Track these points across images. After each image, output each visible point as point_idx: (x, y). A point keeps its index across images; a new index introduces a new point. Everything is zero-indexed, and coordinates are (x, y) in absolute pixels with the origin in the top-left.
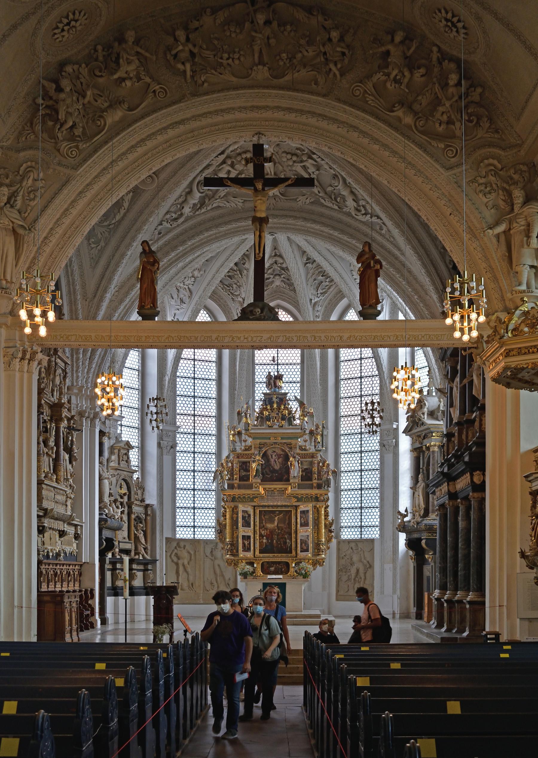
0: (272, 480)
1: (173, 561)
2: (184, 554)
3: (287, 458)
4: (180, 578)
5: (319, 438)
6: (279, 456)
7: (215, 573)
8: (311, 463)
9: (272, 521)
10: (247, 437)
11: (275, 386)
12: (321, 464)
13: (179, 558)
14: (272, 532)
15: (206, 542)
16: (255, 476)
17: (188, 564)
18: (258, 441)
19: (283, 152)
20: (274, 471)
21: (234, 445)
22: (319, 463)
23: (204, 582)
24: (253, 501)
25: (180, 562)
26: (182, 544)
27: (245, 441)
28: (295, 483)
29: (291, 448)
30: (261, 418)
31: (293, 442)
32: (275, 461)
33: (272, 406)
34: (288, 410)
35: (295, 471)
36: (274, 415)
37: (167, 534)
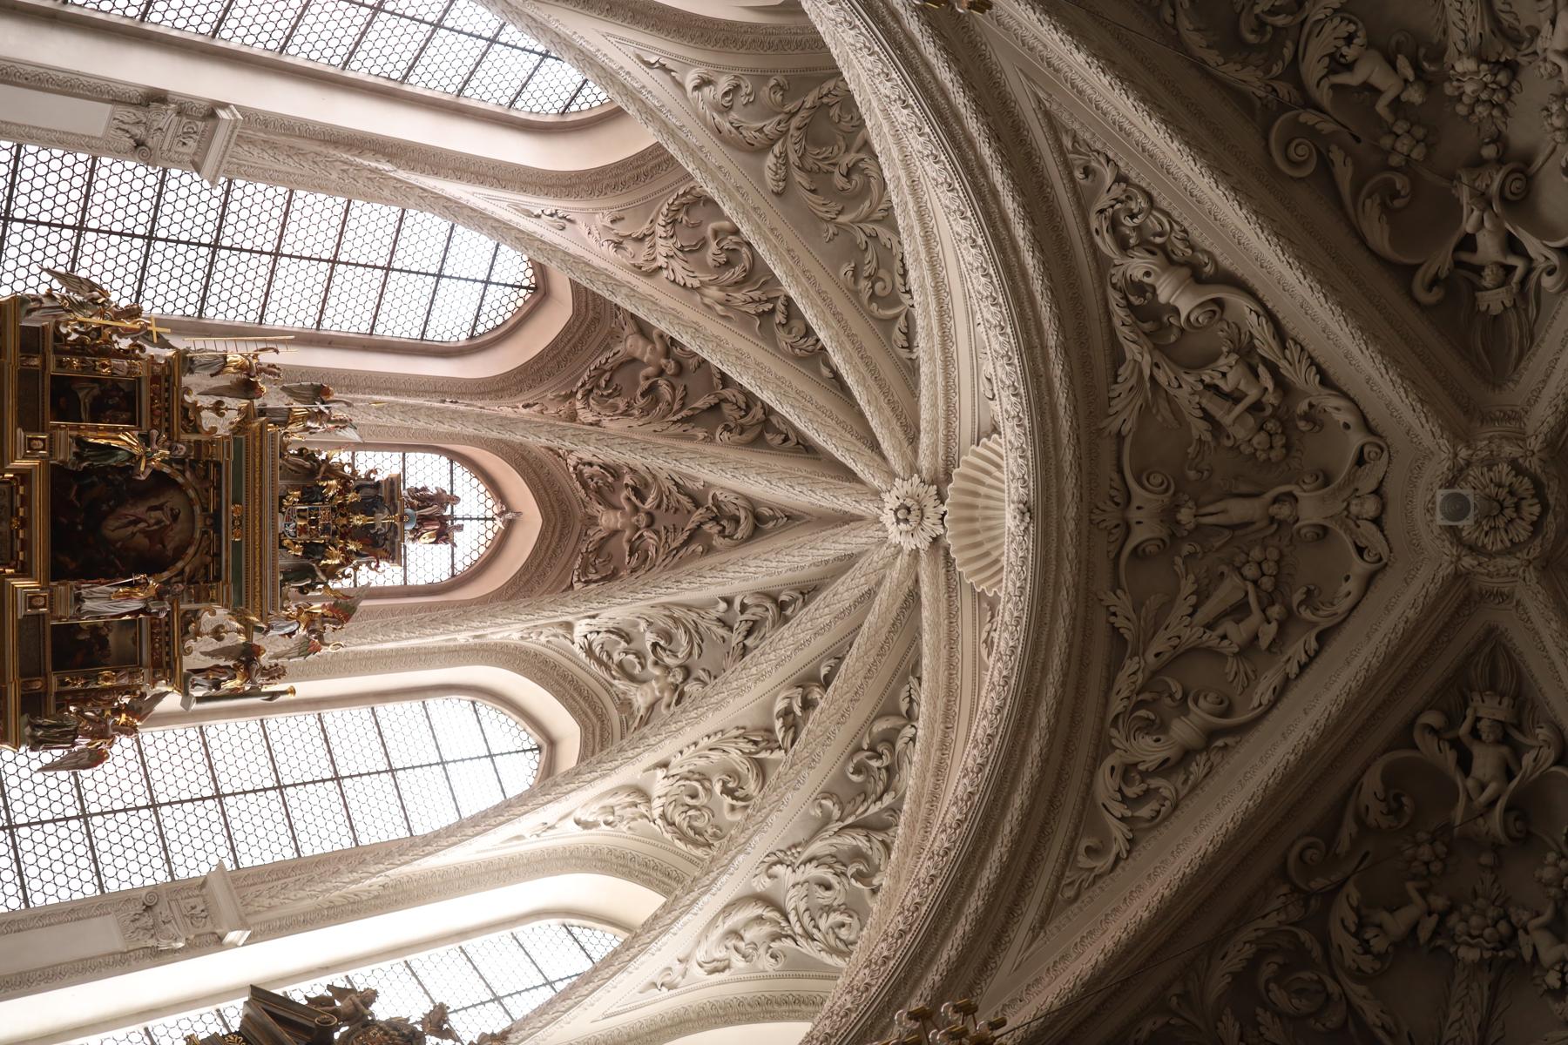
5: (230, 685)
8: (129, 662)
10: (233, 416)
11: (423, 520)
12: (126, 700)
16: (80, 442)
18: (226, 458)
19: (1282, 555)
21: (206, 366)
22: (126, 690)
27: (217, 408)
28: (50, 601)
29: (191, 580)
30: (310, 474)
31: (225, 588)
33: (356, 508)
34: (341, 565)
35: (106, 602)
36: (324, 514)
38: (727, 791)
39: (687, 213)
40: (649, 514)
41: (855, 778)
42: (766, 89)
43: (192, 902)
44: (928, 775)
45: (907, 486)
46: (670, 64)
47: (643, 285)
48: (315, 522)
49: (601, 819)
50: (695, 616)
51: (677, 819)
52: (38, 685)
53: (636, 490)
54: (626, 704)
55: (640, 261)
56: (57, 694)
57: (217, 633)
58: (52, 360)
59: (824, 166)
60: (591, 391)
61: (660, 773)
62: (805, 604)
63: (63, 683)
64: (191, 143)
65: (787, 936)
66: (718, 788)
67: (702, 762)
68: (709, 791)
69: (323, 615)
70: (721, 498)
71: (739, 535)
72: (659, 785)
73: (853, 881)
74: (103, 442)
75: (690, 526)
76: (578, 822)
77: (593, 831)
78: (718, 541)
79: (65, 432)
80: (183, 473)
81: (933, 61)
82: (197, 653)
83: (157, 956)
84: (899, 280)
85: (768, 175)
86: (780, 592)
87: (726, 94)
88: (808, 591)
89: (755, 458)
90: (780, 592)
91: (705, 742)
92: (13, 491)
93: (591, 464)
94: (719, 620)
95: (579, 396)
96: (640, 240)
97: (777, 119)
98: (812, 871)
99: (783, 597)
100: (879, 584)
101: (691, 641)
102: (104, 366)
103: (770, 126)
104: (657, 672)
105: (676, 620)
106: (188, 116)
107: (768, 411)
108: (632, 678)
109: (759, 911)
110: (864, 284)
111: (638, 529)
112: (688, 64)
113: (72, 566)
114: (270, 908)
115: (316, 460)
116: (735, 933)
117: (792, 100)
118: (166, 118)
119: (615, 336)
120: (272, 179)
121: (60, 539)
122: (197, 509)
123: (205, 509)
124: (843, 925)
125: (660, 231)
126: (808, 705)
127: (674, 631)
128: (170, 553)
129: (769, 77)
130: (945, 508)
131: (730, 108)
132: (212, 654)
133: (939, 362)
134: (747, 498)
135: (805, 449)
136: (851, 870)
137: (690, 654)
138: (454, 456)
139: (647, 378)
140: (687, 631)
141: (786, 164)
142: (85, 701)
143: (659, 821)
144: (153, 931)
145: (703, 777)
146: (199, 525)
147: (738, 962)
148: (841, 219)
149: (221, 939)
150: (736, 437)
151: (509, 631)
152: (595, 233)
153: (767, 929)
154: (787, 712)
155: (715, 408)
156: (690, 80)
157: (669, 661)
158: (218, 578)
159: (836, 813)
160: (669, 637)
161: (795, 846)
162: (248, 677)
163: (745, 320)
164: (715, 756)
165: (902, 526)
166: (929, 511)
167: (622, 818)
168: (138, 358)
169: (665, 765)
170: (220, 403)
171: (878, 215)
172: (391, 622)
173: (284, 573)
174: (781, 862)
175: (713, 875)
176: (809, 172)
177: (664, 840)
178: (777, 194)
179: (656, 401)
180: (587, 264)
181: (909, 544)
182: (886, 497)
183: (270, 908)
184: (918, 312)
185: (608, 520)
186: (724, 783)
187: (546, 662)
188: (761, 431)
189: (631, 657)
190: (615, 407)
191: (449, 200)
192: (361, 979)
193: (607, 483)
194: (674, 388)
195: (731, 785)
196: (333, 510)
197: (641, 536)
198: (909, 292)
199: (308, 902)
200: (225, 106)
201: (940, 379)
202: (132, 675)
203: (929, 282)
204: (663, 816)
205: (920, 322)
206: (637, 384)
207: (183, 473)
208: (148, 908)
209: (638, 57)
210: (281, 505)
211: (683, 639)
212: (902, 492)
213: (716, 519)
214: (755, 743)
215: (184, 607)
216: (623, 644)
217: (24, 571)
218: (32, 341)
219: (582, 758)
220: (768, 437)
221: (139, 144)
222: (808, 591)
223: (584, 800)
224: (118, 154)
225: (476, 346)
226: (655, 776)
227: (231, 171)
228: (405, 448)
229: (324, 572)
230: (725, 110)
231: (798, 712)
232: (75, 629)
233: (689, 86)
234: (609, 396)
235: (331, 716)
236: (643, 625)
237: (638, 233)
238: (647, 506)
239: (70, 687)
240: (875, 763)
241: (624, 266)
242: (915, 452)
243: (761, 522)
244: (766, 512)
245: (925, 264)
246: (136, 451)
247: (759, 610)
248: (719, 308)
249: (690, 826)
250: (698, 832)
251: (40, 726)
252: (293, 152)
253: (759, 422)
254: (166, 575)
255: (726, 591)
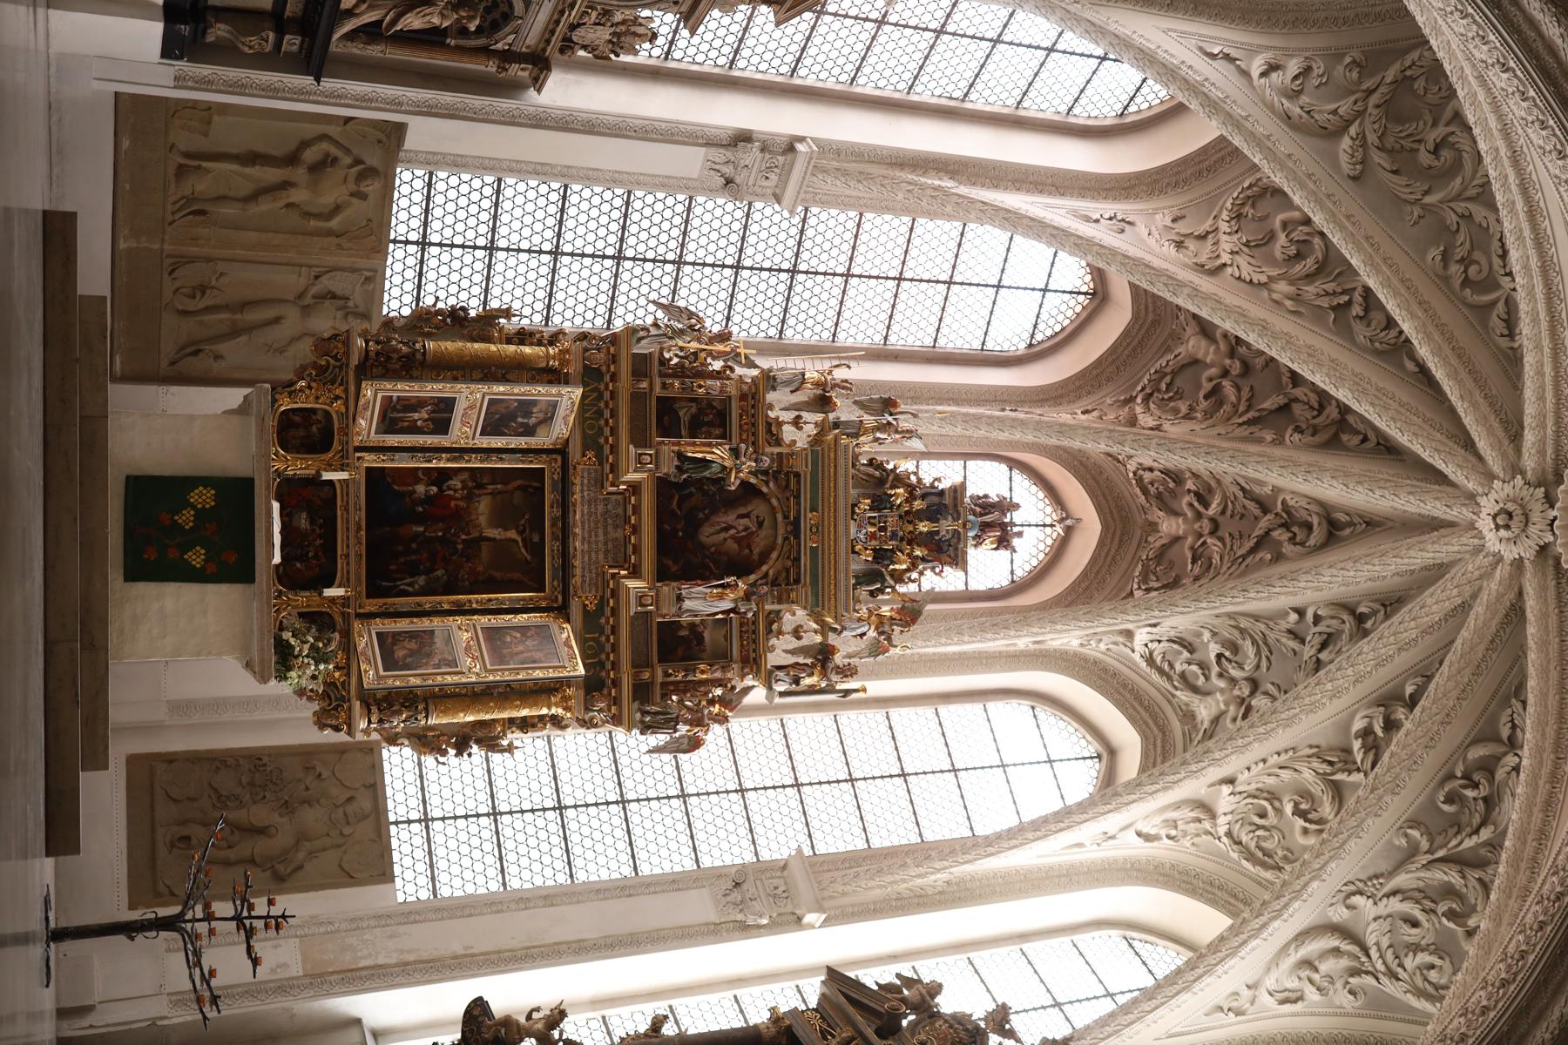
0: (663, 514)
1: (305, 144)
2: (332, 192)
3: (741, 568)
4: (235, 167)
5: (807, 681)
6: (745, 541)
7: (245, 305)
8: (721, 658)
9: (499, 520)
10: (810, 430)
11: (985, 527)
12: (719, 692)
13: (318, 168)
14: (459, 518)
15: (374, 280)
17: (288, 205)
18: (804, 468)
20: (694, 525)
22: (720, 683)
23: (209, 260)
24: (585, 448)
25: (299, 174)
26: (372, 187)
28: (657, 601)
29: (775, 583)
30: (879, 481)
31: (803, 591)
32: (726, 529)
34: (908, 570)
35: (702, 602)
36: (892, 520)
37: (421, 133)
38: (1298, 812)
39: (1253, 206)
40: (1213, 520)
41: (1446, 808)
42: (1340, 68)
43: (775, 882)
44: (1536, 810)
45: (1508, 489)
46: (1234, 53)
47: (1206, 284)
48: (883, 529)
49: (1163, 833)
50: (1263, 627)
51: (1244, 839)
52: (646, 676)
53: (1197, 494)
54: (1189, 716)
55: (1202, 259)
56: (663, 684)
57: (797, 633)
58: (658, 381)
59: (1407, 144)
60: (1151, 395)
61: (1226, 789)
62: (1387, 617)
63: (667, 675)
64: (773, 177)
65: (1367, 973)
66: (1289, 809)
67: (1271, 781)
68: (1279, 812)
69: (891, 618)
70: (1291, 503)
71: (1311, 542)
72: (1225, 801)
73: (1444, 920)
74: (700, 455)
75: (1258, 532)
76: (1139, 834)
77: (1155, 844)
78: (1288, 549)
79: (668, 447)
80: (767, 483)
81: (1539, 16)
82: (780, 651)
83: (745, 930)
84: (1497, 262)
85: (1344, 159)
86: (1359, 603)
87: (1296, 77)
88: (1391, 603)
89: (1330, 461)
90: (1359, 603)
91: (1275, 759)
92: (626, 501)
93: (1151, 470)
94: (1290, 631)
95: (1139, 400)
96: (1202, 237)
97: (1353, 98)
98: (1396, 905)
99: (1362, 609)
100: (1474, 596)
101: (1258, 653)
102: (700, 387)
103: (1345, 107)
104: (1222, 684)
105: (1242, 631)
106: (770, 152)
107: (1344, 410)
108: (1195, 690)
109: (1335, 942)
110: (1455, 269)
111: (1201, 536)
112: (1253, 51)
113: (674, 569)
114: (844, 894)
115: (885, 470)
116: (1308, 964)
117: (1371, 75)
118: (751, 156)
119: (1176, 337)
120: (844, 205)
121: (666, 544)
122: (779, 516)
123: (786, 517)
124: (1432, 967)
125: (1224, 227)
126: (1391, 725)
127: (1240, 642)
128: (756, 557)
129: (1344, 55)
130: (1555, 513)
131: (1300, 92)
132: (792, 652)
133: (1547, 350)
134: (1321, 503)
135: (1387, 450)
136: (1442, 908)
137: (1258, 667)
138: (1013, 464)
139: (1210, 380)
140: (1254, 642)
141: (1364, 145)
142: (685, 692)
143: (1224, 839)
144: (741, 905)
145: (1273, 796)
146: (781, 531)
147: (1312, 995)
148: (1428, 199)
149: (800, 919)
150: (1308, 439)
151: (1068, 638)
152: (1155, 233)
153: (1345, 962)
154: (1367, 732)
155: (1284, 409)
156: (1256, 66)
157: (1235, 673)
158: (797, 581)
159: (1425, 845)
160: (1235, 649)
161: (1377, 877)
162: (824, 675)
163: (1317, 314)
164: (1286, 775)
165: (1503, 533)
166: (1535, 516)
167: (1185, 834)
168: (729, 378)
169: (1231, 781)
170: (799, 417)
171: (1472, 192)
172: (953, 626)
173: (856, 577)
174: (1361, 893)
175: (1284, 900)
176: (1390, 152)
177: (1229, 859)
178: (1354, 178)
179: (1220, 403)
180: (1147, 266)
181: (1510, 553)
182: (1483, 501)
183: (844, 894)
184: (1521, 297)
185: (1169, 526)
186: (1296, 804)
187: (1105, 670)
188: (1337, 432)
189: (1194, 668)
190: (1176, 411)
191: (1008, 211)
192: (928, 971)
193: (1168, 489)
194: (1239, 389)
195: (1303, 806)
196: (901, 517)
197: (1204, 543)
198: (1510, 274)
199: (878, 891)
200: (802, 139)
201: (1548, 369)
202: (724, 669)
203: (1534, 262)
204: (1229, 834)
205: (1523, 307)
206: (1199, 386)
207: (767, 483)
208: (737, 885)
209: (1201, 49)
210: (853, 512)
211: (1249, 650)
212: (1503, 495)
213: (1286, 526)
214: (1331, 763)
215: (768, 607)
216: (1186, 654)
217: (635, 573)
218: (641, 365)
219: (1143, 769)
220: (1344, 437)
221: (729, 181)
222: (1391, 603)
223: (1146, 812)
224: (711, 192)
225: (1035, 354)
226: (1220, 791)
227: (809, 200)
228: (966, 456)
229: (892, 576)
230: (1294, 95)
231: (1380, 733)
232: (676, 626)
233: (1255, 74)
234: (1170, 399)
235: (897, 714)
236: (1207, 636)
237: (1201, 230)
238: (1211, 512)
239: (672, 679)
240: (1470, 793)
241: (1186, 265)
242: (1518, 451)
243: (1338, 529)
244: (1342, 517)
245: (1529, 242)
246: (728, 464)
247: (1334, 622)
248: (1288, 303)
249: (1258, 847)
250: (1266, 853)
251: (648, 713)
252: (864, 177)
253: (1334, 422)
254: (752, 577)
255: (1297, 601)
